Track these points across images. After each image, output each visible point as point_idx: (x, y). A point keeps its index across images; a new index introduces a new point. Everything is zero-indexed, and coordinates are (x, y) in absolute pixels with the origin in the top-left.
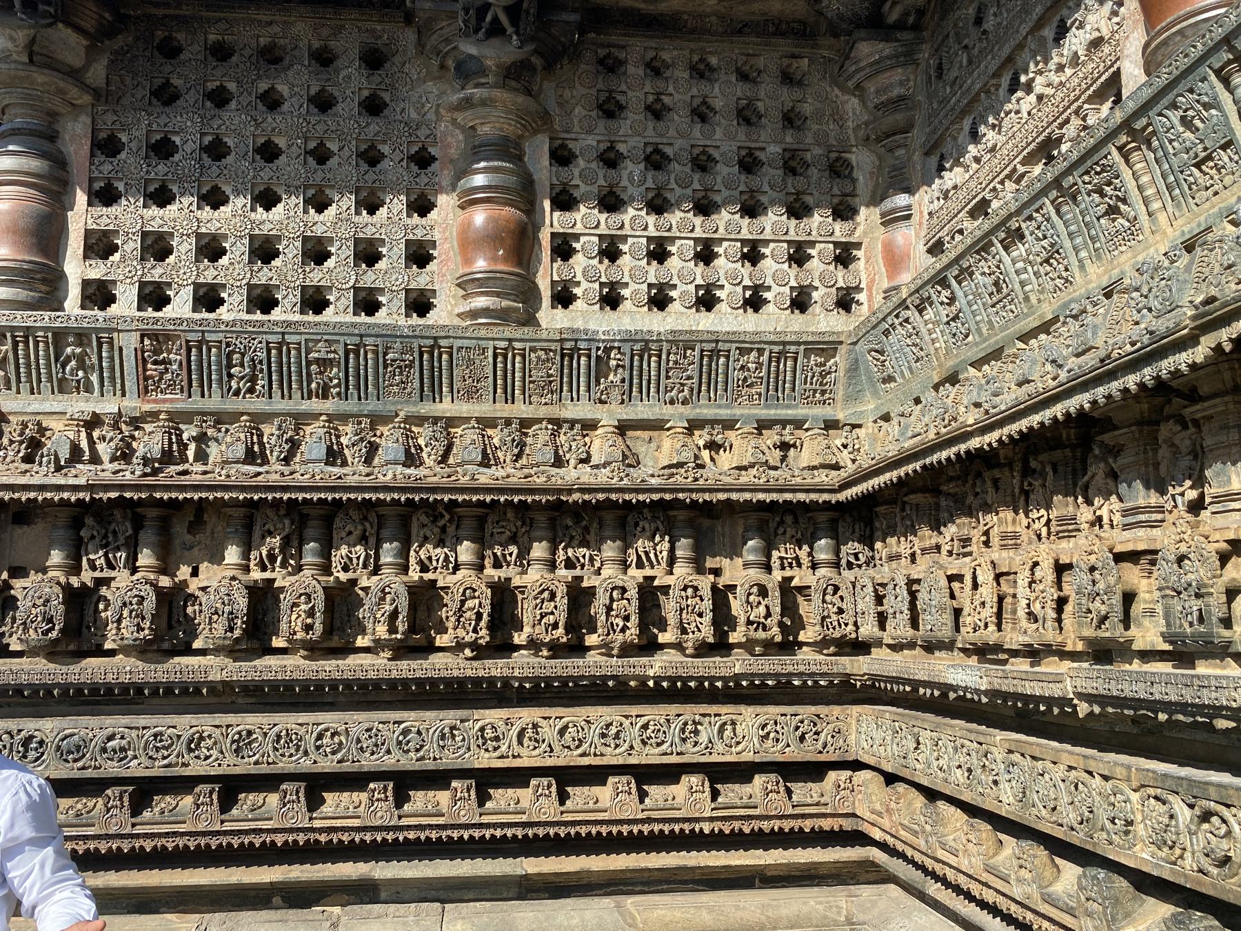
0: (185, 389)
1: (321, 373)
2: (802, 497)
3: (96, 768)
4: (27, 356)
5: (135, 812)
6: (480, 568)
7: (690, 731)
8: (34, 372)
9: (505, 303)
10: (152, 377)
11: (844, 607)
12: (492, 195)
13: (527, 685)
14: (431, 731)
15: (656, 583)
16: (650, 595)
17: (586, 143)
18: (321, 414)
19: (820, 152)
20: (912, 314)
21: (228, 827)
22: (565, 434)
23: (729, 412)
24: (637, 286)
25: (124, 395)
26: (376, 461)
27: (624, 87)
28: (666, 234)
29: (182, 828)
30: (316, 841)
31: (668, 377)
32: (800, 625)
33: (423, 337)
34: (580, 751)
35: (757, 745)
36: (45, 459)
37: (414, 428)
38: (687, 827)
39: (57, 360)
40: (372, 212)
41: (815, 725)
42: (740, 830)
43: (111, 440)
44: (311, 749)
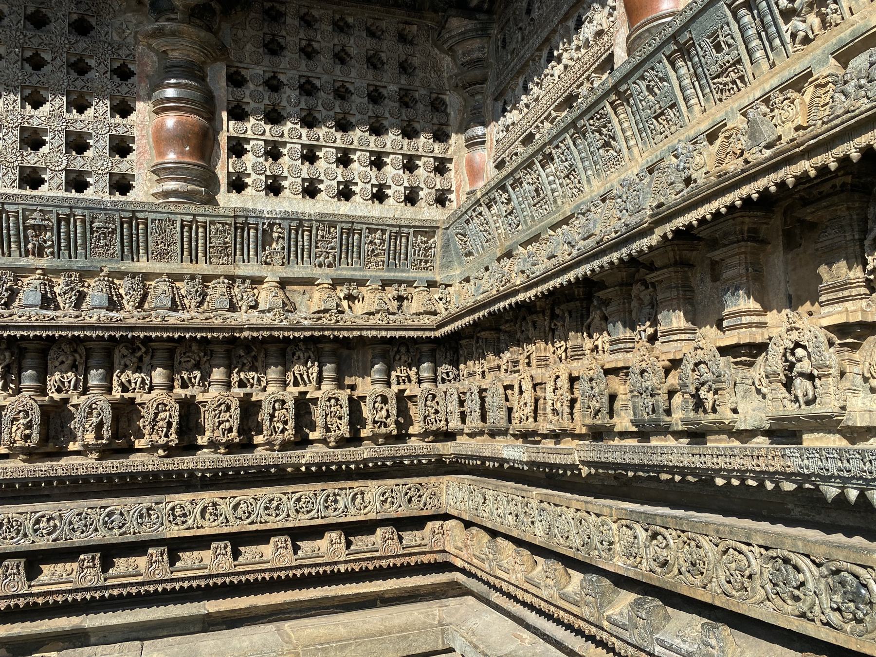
1: (36, 236)
2: (411, 334)
6: (171, 388)
7: (331, 501)
9: (190, 187)
11: (439, 409)
12: (179, 105)
13: (208, 475)
14: (131, 513)
15: (308, 396)
16: (303, 405)
17: (256, 71)
19: (425, 92)
20: (483, 209)
22: (238, 287)
23: (361, 273)
24: (294, 180)
26: (84, 306)
27: (284, 33)
28: (315, 143)
30: (35, 603)
31: (317, 247)
32: (409, 422)
33: (123, 211)
34: (249, 520)
35: (379, 507)
37: (116, 281)
38: (328, 569)
40: (81, 111)
41: (419, 490)
42: (367, 567)
44: (30, 531)
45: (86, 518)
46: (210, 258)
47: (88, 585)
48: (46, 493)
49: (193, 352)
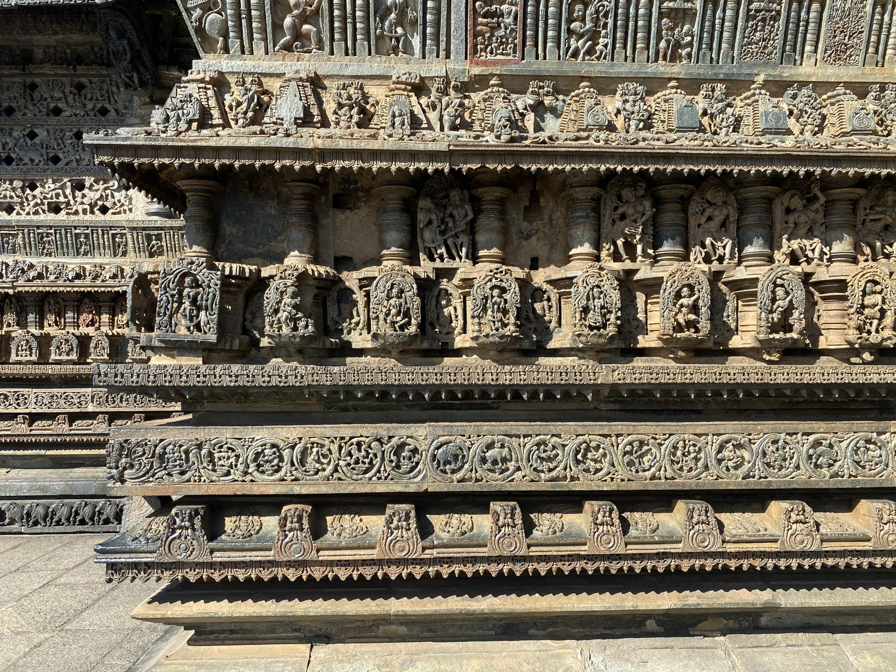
0: (519, 48)
3: (477, 480)
8: (349, 26)
18: (670, 79)
21: (633, 549)
25: (448, 56)
29: (584, 550)
36: (398, 120)
39: (375, 14)
43: (448, 106)
44: (712, 462)
45: (784, 448)
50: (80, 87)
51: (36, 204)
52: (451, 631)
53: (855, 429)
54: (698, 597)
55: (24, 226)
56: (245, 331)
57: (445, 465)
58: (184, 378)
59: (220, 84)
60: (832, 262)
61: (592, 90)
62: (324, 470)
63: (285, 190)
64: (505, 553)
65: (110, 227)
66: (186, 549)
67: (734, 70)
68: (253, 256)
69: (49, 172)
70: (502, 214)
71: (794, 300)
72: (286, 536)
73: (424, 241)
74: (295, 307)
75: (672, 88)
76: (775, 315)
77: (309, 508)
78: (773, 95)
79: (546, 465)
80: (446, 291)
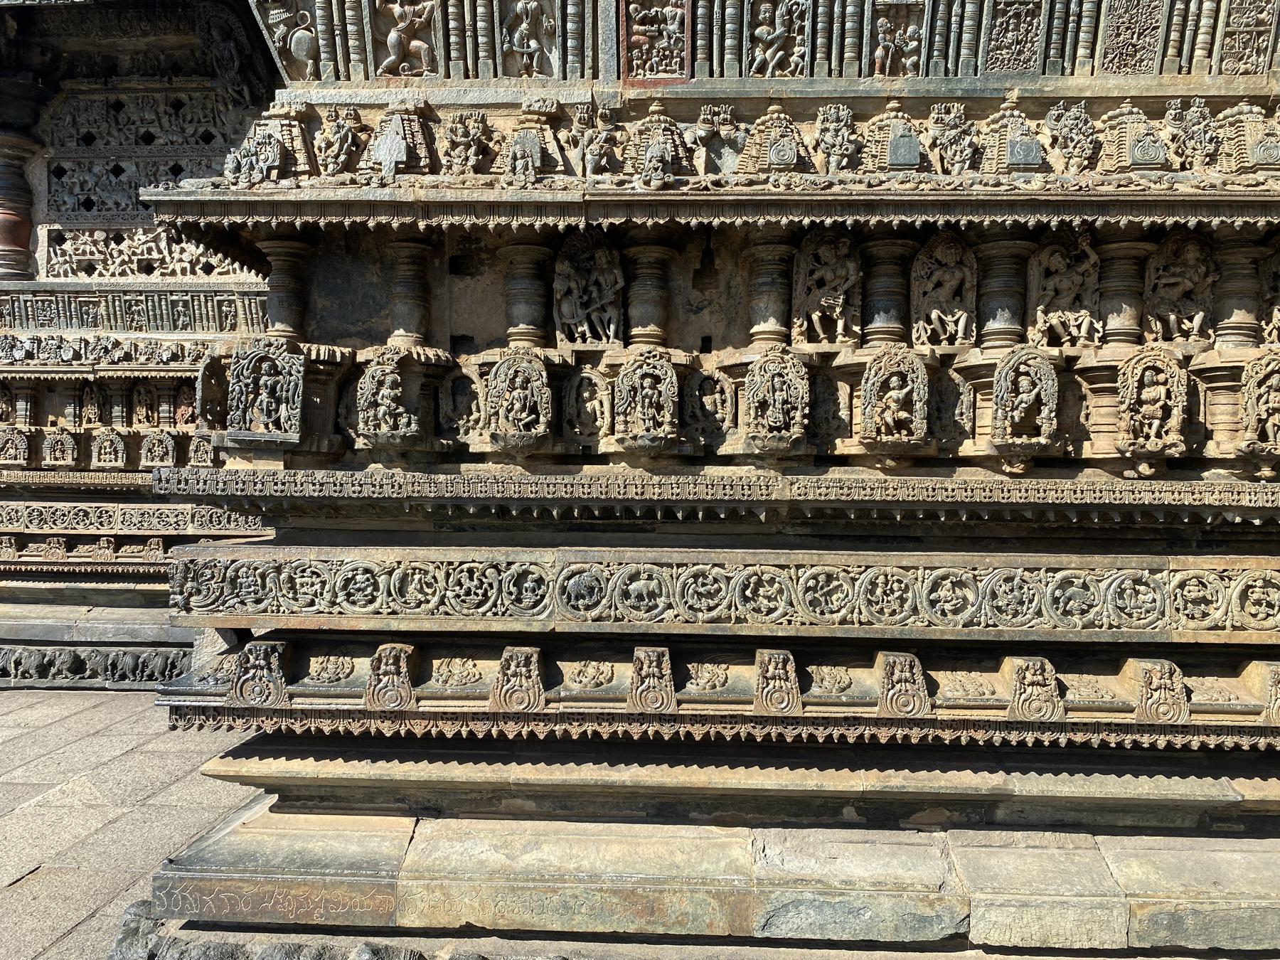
0: (687, 63)
3: (617, 619)
4: (461, 17)
5: (679, 686)
6: (1140, 340)
8: (469, 41)
10: (638, 45)
13: (1257, 522)
18: (889, 99)
21: (812, 712)
25: (595, 76)
29: (749, 710)
36: (520, 163)
39: (501, 24)
43: (591, 141)
44: (923, 605)
45: (1021, 588)
46: (1222, 60)
47: (1034, 717)
48: (919, 533)
49: (1185, 264)
50: (178, 105)
51: (123, 263)
52: (591, 809)
53: (1119, 565)
54: (904, 778)
55: (107, 291)
56: (339, 430)
57: (577, 599)
58: (259, 486)
59: (308, 119)
60: (1107, 342)
61: (782, 116)
62: (428, 602)
63: (389, 251)
64: (649, 711)
65: (216, 292)
66: (261, 692)
67: (978, 84)
68: (350, 335)
69: (139, 219)
70: (664, 281)
71: (1043, 394)
72: (380, 681)
73: (561, 316)
74: (395, 399)
75: (892, 110)
76: (1016, 413)
77: (410, 649)
78: (1031, 116)
79: (705, 602)
80: (590, 380)
